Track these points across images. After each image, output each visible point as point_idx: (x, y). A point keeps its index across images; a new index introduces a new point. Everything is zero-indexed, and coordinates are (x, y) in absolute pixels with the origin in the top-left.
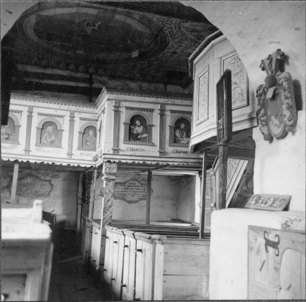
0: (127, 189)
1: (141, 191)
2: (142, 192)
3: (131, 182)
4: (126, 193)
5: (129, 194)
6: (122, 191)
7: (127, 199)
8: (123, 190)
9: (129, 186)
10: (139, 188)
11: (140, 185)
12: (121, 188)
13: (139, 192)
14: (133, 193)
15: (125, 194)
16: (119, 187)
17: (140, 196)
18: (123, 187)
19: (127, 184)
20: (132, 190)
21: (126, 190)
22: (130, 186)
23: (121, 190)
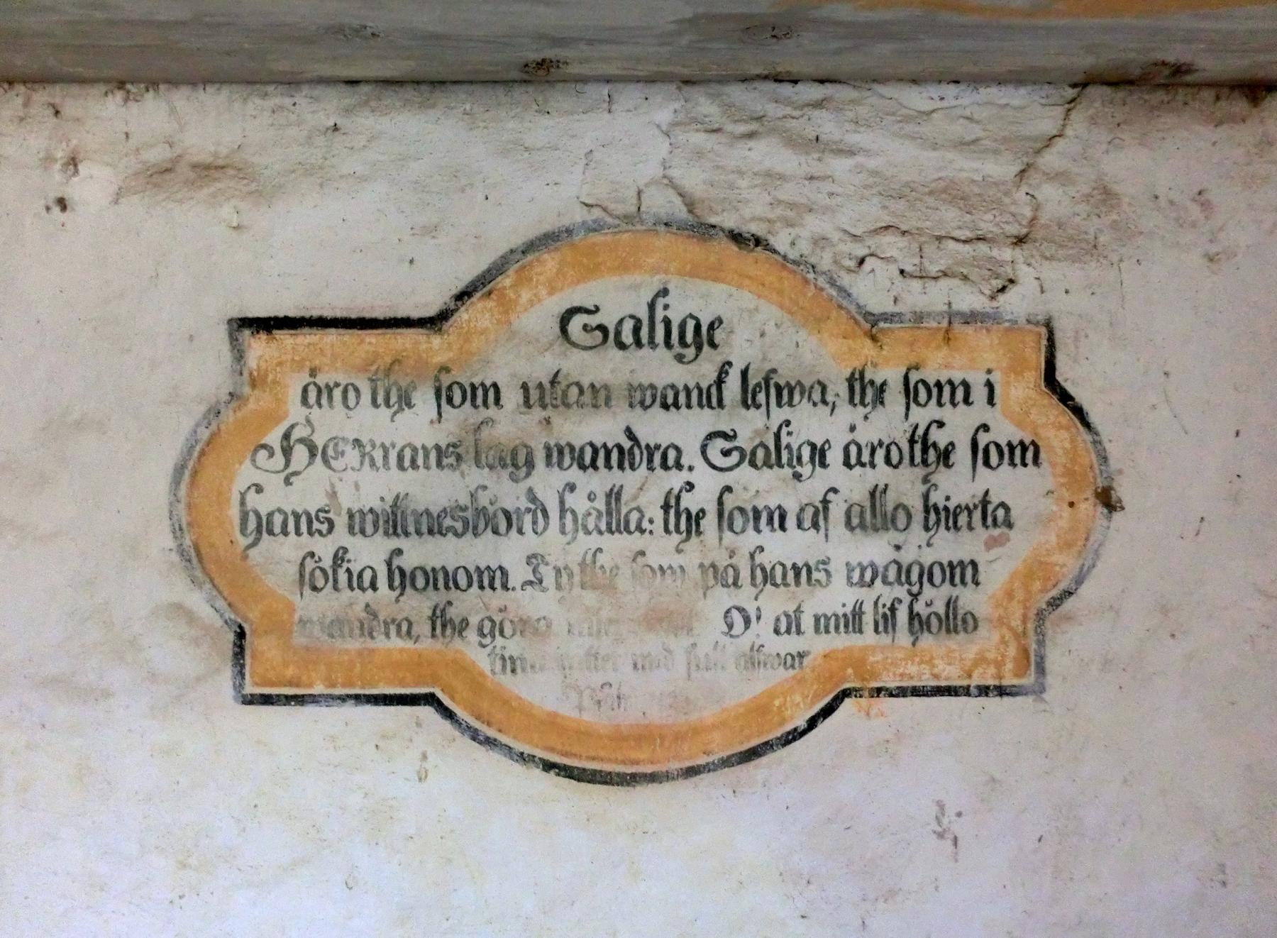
0: (517, 461)
1: (855, 486)
2: (875, 514)
3: (618, 299)
4: (509, 552)
5: (591, 573)
6: (393, 521)
7: (540, 691)
8: (435, 489)
9: (546, 395)
10: (809, 423)
11: (824, 354)
12: (373, 450)
13: (818, 515)
14: (661, 548)
15: (493, 578)
16: (330, 422)
17: (837, 596)
18: (420, 424)
19: (513, 341)
20: (646, 489)
21: (509, 494)
22: (598, 396)
23: (373, 488)
